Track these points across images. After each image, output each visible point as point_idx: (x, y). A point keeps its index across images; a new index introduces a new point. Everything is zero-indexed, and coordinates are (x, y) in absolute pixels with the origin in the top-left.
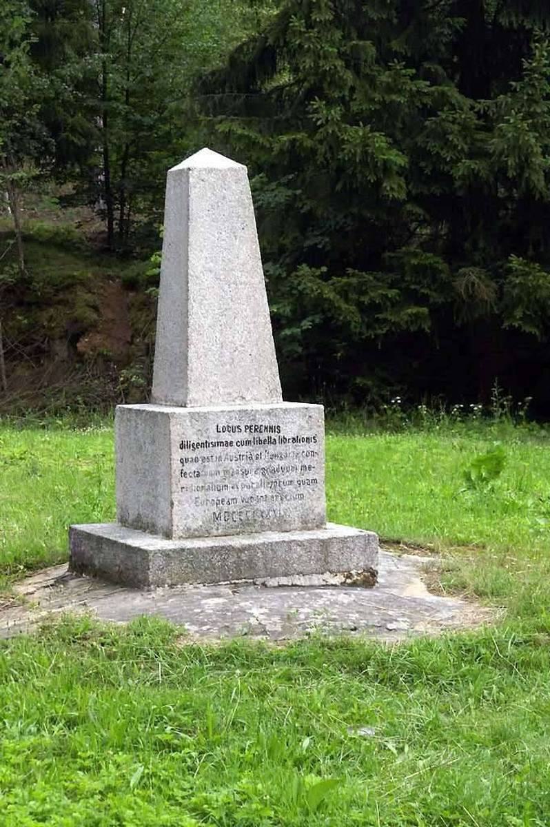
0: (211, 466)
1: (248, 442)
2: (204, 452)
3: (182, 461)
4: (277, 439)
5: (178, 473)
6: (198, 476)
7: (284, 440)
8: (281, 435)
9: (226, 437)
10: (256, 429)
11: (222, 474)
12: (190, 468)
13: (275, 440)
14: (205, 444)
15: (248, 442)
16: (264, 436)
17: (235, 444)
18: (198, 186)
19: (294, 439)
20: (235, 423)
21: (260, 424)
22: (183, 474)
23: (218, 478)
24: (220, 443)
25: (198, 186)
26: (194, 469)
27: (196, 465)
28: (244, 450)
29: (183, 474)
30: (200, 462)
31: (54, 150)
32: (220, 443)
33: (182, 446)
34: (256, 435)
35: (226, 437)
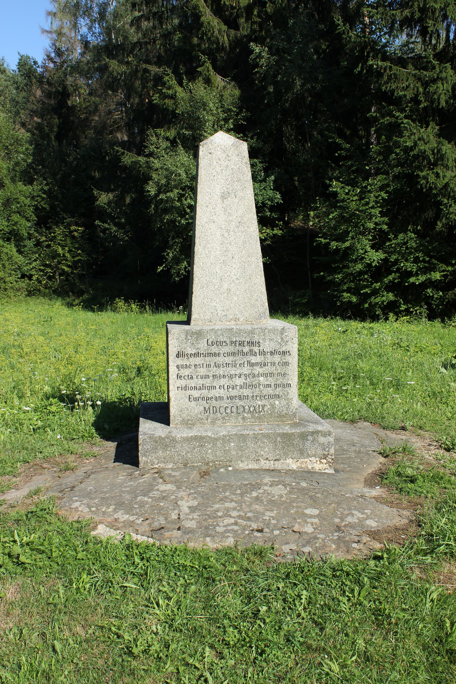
1: (233, 354)
2: (198, 360)
3: (178, 367)
4: (257, 351)
5: (175, 376)
6: (192, 378)
7: (263, 353)
8: (261, 348)
9: (214, 349)
10: (240, 344)
11: (211, 378)
12: (185, 372)
13: (256, 353)
14: (197, 355)
15: (233, 354)
16: (246, 349)
17: (222, 355)
19: (271, 352)
20: (221, 339)
21: (243, 339)
22: (179, 377)
24: (210, 354)
25: (206, 158)
26: (187, 374)
28: (229, 360)
29: (179, 377)
30: (193, 367)
31: (162, 196)
32: (210, 354)
33: (178, 356)
34: (240, 348)
35: (214, 349)
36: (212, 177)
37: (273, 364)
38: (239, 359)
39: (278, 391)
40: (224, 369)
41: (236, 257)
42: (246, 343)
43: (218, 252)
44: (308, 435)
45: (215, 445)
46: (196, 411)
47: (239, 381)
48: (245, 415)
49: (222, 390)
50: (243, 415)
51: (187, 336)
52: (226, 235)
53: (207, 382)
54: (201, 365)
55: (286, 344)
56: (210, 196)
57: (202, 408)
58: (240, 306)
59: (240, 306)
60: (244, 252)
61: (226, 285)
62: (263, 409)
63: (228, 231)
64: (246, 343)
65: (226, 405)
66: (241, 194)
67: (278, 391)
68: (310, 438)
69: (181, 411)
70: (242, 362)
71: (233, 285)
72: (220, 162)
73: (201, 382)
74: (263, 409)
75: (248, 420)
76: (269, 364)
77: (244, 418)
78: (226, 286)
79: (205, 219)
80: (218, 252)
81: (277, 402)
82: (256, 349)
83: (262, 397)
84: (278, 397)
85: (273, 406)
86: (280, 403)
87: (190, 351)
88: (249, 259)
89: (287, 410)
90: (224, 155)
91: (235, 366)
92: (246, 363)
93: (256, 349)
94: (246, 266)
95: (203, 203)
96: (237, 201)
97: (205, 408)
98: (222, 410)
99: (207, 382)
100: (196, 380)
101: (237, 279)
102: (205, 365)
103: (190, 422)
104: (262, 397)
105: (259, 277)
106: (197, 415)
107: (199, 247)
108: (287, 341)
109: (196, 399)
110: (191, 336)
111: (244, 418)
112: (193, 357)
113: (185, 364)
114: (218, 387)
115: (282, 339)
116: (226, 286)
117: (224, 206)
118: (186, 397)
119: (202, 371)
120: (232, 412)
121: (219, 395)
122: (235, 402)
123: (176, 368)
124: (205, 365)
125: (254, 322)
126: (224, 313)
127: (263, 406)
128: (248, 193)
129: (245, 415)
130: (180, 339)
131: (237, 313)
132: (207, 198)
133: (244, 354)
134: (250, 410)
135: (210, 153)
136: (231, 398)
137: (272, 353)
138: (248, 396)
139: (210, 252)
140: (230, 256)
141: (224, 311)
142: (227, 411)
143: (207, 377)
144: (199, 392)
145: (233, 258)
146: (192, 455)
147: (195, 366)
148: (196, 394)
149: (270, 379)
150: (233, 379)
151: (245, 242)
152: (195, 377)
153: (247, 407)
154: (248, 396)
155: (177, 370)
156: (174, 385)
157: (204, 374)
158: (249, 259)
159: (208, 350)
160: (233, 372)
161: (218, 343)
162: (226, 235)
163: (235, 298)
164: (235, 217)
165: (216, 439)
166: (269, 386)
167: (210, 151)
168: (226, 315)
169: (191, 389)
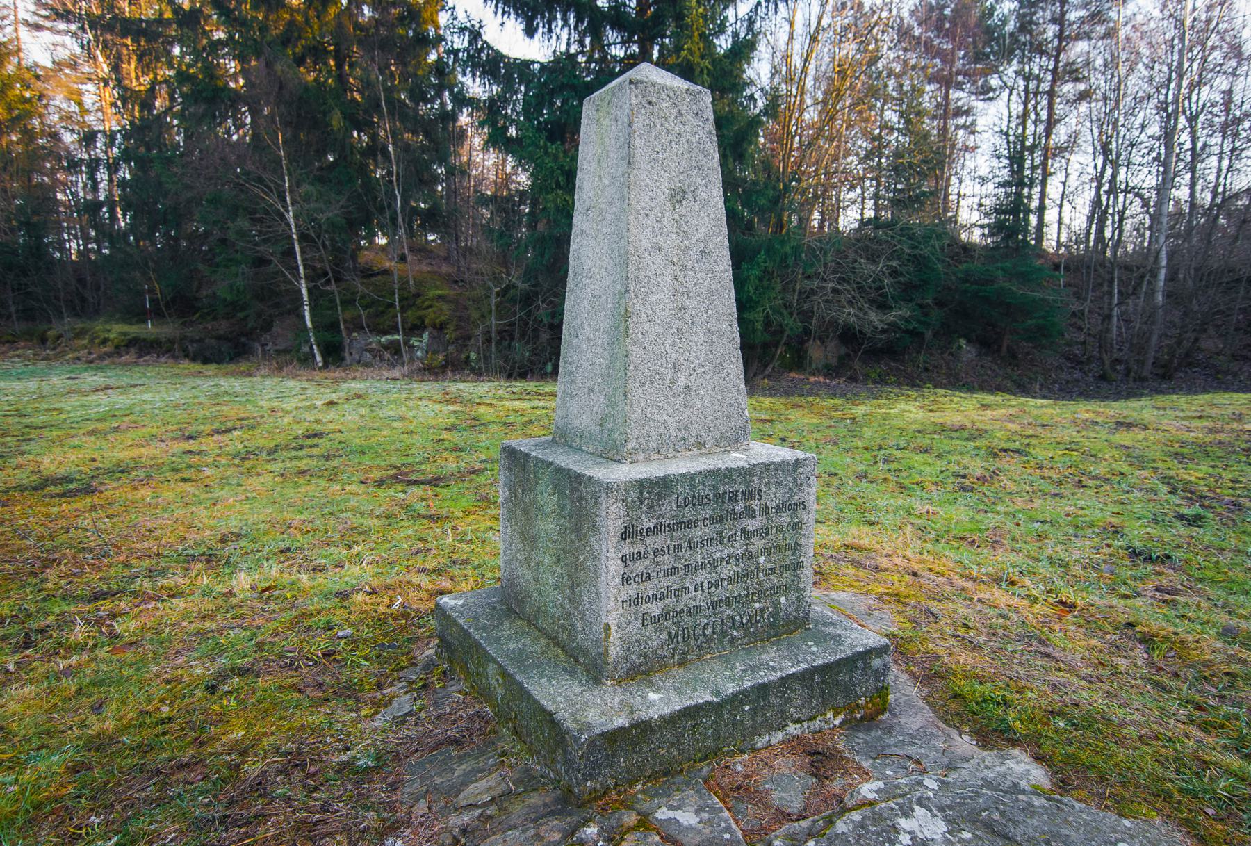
0: (667, 560)
1: (720, 519)
2: (660, 541)
7: (765, 511)
8: (763, 502)
9: (688, 515)
11: (682, 572)
12: (639, 567)
13: (754, 511)
18: (643, 112)
22: (626, 580)
23: (677, 578)
24: (680, 525)
26: (639, 571)
27: (647, 562)
30: (651, 556)
36: (654, 155)
37: (779, 528)
38: (727, 528)
39: (786, 578)
40: (704, 551)
41: (697, 320)
42: (740, 496)
43: (668, 310)
44: (857, 660)
45: (720, 716)
46: (655, 643)
47: (726, 571)
48: (735, 633)
49: (700, 592)
50: (732, 635)
51: (641, 493)
52: (680, 276)
53: (673, 582)
54: (666, 549)
55: (800, 490)
56: (651, 194)
57: (664, 636)
58: (705, 418)
59: (705, 418)
60: (710, 312)
61: (683, 378)
62: (762, 616)
63: (683, 269)
64: (740, 496)
65: (706, 621)
66: (704, 195)
67: (786, 578)
68: (860, 664)
69: (628, 650)
70: (733, 532)
71: (693, 377)
72: (667, 125)
73: (664, 583)
74: (762, 616)
75: (740, 642)
76: (774, 530)
77: (733, 640)
78: (682, 380)
79: (643, 242)
80: (668, 310)
81: (783, 600)
82: (755, 504)
83: (761, 593)
84: (785, 589)
85: (776, 605)
86: (787, 599)
87: (648, 522)
88: (719, 326)
89: (797, 610)
90: (674, 111)
91: (722, 543)
92: (739, 533)
93: (755, 504)
94: (715, 340)
95: (639, 207)
96: (697, 208)
97: (670, 634)
98: (698, 631)
99: (673, 582)
100: (656, 581)
101: (701, 366)
102: (671, 548)
103: (643, 668)
104: (761, 593)
105: (734, 360)
106: (654, 652)
107: (635, 301)
108: (801, 484)
109: (654, 621)
110: (649, 492)
111: (733, 640)
112: (651, 534)
113: (637, 550)
114: (692, 588)
115: (795, 480)
116: (682, 380)
117: (676, 216)
118: (637, 619)
119: (667, 560)
120: (714, 633)
121: (694, 603)
122: (720, 612)
123: (619, 562)
124: (671, 548)
125: (728, 448)
126: (680, 435)
127: (763, 610)
128: (715, 193)
129: (735, 633)
130: (630, 499)
131: (702, 433)
132: (647, 198)
133: (736, 517)
134: (742, 622)
135: (650, 103)
136: (714, 605)
137: (779, 509)
138: (740, 595)
139: (654, 311)
140: (688, 319)
141: (680, 430)
142: (707, 633)
143: (673, 571)
144: (661, 604)
145: (693, 323)
146: (678, 750)
147: (655, 551)
148: (655, 609)
149: (774, 558)
150: (718, 568)
151: (710, 291)
152: (654, 574)
153: (737, 618)
154: (740, 595)
155: (622, 566)
156: (616, 598)
157: (671, 565)
158: (719, 326)
159: (677, 516)
160: (717, 555)
161: (695, 500)
162: (680, 276)
163: (699, 404)
164: (694, 241)
165: (720, 706)
166: (772, 570)
167: (650, 99)
168: (683, 439)
169: (648, 600)
